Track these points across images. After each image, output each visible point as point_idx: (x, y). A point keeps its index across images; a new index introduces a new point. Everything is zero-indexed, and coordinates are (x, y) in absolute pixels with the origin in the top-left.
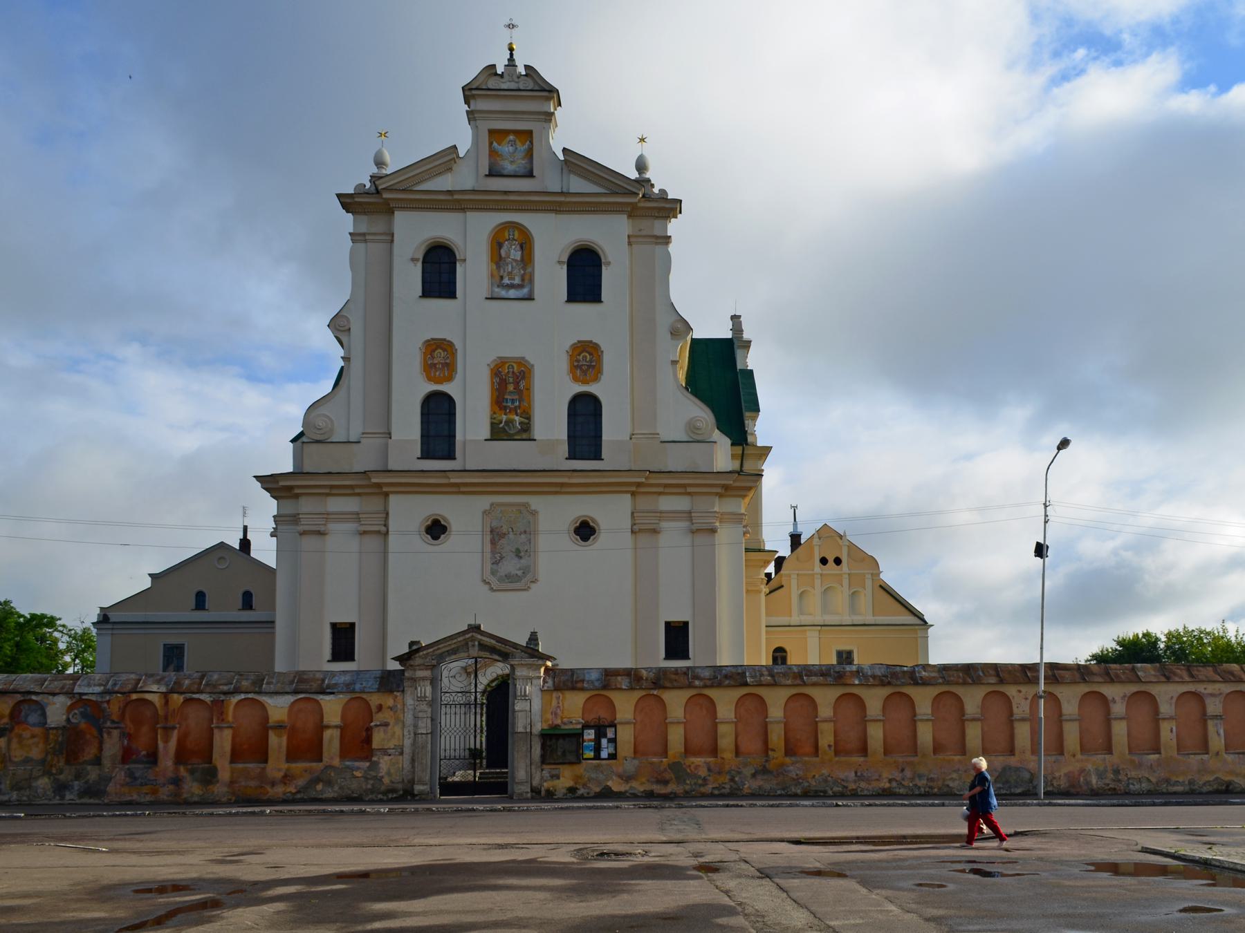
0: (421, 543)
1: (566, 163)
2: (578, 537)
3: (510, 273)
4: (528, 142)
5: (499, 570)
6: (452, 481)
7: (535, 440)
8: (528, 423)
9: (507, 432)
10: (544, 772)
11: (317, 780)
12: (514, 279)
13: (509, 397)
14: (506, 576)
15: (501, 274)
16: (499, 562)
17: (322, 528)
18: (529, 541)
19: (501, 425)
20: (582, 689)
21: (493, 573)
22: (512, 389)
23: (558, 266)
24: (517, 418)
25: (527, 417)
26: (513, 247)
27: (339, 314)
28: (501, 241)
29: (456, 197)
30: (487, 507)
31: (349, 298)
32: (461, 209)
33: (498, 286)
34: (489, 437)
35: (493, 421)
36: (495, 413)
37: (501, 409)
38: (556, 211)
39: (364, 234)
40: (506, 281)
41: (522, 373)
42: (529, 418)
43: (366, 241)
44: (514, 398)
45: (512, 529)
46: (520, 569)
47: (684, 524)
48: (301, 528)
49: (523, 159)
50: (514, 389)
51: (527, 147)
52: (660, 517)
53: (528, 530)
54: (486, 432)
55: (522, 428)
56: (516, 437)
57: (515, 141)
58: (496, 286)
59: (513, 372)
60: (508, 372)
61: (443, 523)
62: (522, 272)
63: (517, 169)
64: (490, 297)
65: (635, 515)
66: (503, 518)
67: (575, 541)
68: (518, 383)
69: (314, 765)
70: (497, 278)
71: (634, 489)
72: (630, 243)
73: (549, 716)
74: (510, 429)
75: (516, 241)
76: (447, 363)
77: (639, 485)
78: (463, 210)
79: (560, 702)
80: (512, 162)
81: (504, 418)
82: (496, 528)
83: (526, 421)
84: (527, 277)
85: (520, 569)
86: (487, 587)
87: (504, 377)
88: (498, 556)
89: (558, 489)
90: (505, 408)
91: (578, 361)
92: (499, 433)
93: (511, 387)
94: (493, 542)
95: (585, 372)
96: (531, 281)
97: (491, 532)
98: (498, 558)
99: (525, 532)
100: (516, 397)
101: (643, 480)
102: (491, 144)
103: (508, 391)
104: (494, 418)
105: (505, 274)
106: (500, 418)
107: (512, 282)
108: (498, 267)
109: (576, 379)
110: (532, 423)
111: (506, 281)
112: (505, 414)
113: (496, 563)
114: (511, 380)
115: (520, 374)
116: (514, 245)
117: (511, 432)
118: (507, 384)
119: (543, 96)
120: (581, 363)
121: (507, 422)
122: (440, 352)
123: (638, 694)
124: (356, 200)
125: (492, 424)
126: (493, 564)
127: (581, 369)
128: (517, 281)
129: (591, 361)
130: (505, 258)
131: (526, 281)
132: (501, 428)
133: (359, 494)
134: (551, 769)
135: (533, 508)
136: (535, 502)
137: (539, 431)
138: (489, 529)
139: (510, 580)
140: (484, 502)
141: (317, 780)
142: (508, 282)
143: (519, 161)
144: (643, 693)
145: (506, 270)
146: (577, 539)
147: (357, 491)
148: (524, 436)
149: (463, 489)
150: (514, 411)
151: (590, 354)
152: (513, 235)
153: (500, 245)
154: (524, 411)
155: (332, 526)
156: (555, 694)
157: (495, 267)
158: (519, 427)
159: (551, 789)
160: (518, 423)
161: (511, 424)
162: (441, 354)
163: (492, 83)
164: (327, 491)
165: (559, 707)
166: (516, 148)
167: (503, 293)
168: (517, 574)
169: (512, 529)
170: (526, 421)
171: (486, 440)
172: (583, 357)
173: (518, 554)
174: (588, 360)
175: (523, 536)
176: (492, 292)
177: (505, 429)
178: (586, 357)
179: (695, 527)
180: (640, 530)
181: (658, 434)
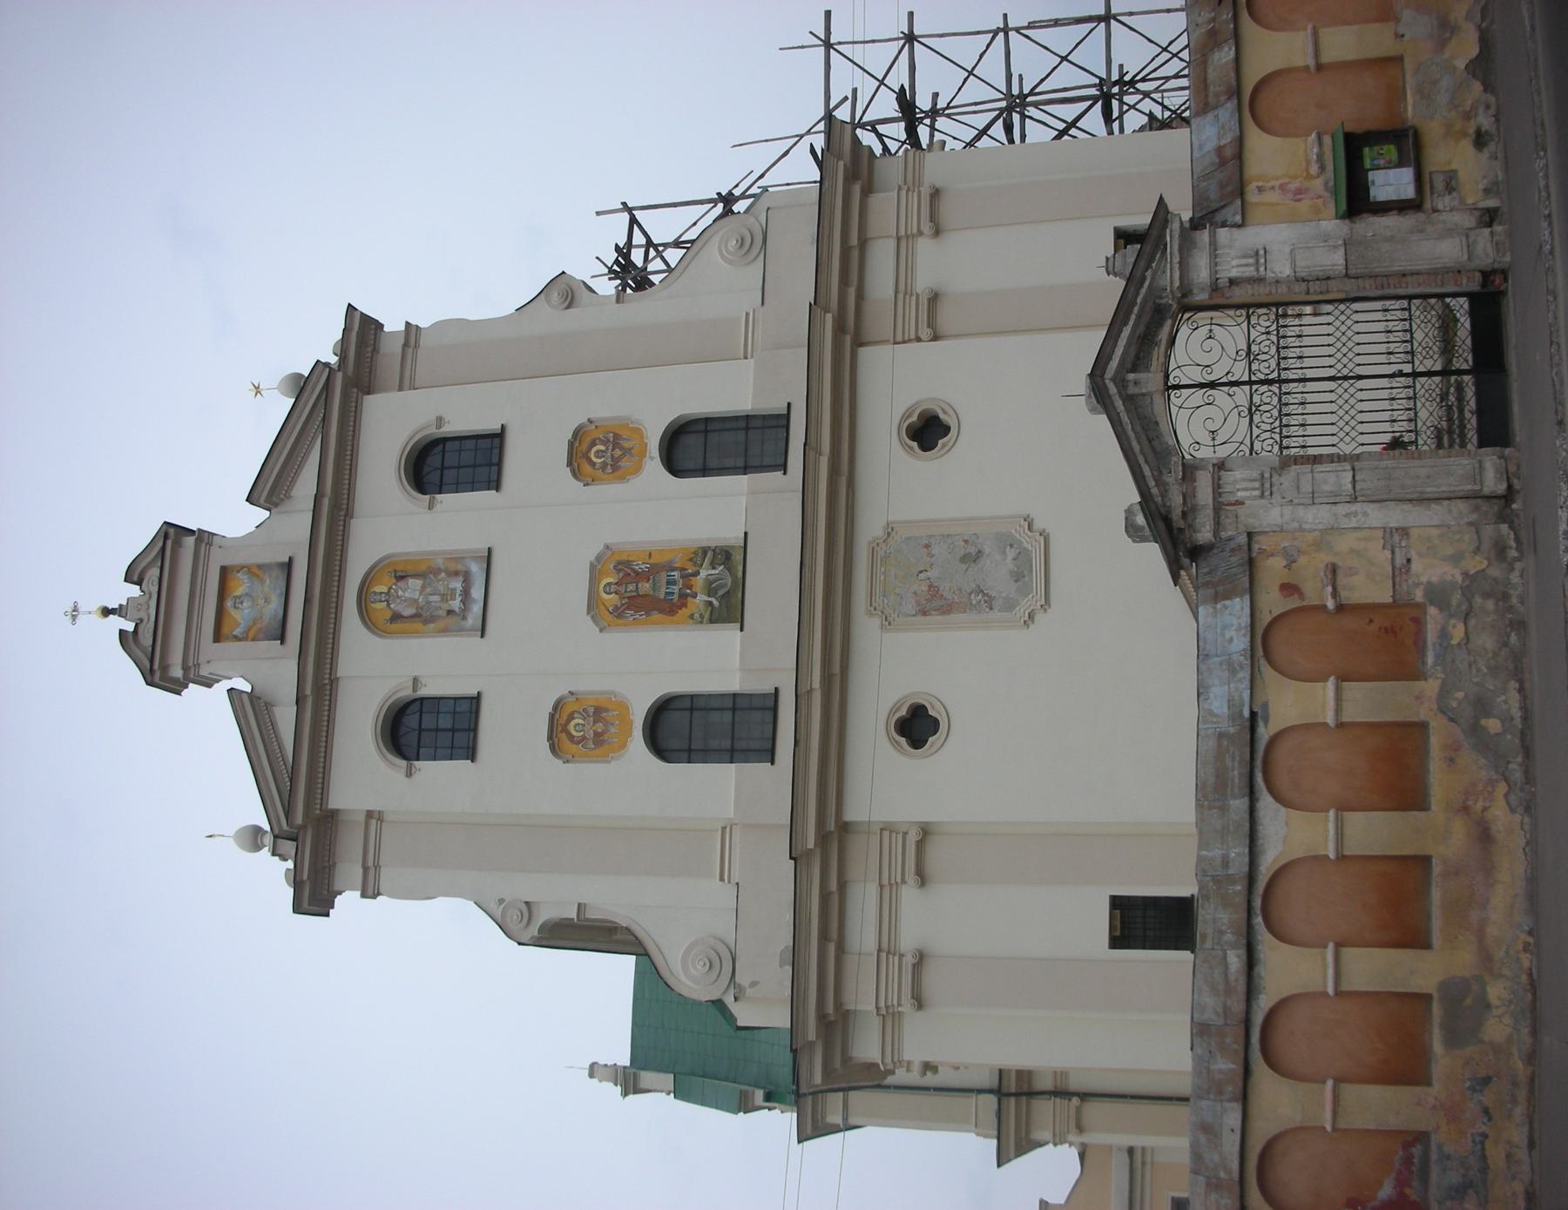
0: (943, 755)
1: (276, 505)
2: (940, 442)
3: (444, 598)
4: (239, 575)
5: (1004, 595)
6: (816, 684)
7: (746, 534)
8: (714, 551)
9: (729, 591)
10: (1440, 207)
11: (1475, 730)
13: (663, 590)
15: (444, 613)
16: (987, 595)
17: (909, 960)
18: (946, 537)
19: (716, 603)
20: (1240, 141)
22: (647, 585)
23: (438, 507)
24: (703, 573)
25: (703, 554)
26: (400, 593)
27: (500, 921)
28: (388, 615)
29: (308, 691)
30: (875, 622)
31: (472, 903)
32: (331, 685)
33: (464, 618)
34: (738, 625)
36: (692, 617)
37: (684, 605)
38: (349, 514)
39: (366, 869)
40: (456, 604)
41: (620, 567)
42: (705, 551)
43: (377, 867)
44: (664, 580)
45: (921, 572)
46: (1004, 553)
47: (924, 246)
48: (907, 1007)
49: (262, 581)
51: (246, 577)
52: (906, 294)
54: (728, 635)
55: (723, 564)
56: (740, 574)
57: (236, 597)
58: (463, 623)
59: (616, 584)
60: (616, 593)
61: (903, 712)
62: (443, 575)
63: (278, 591)
64: (480, 633)
65: (899, 338)
66: (897, 591)
67: (947, 448)
68: (637, 574)
69: (1435, 742)
70: (451, 620)
71: (848, 339)
72: (415, 389)
73: (1305, 205)
74: (725, 585)
75: (390, 588)
76: (594, 713)
77: (840, 329)
78: (334, 681)
79: (1270, 184)
80: (267, 601)
81: (702, 597)
82: (918, 604)
83: (710, 554)
84: (452, 566)
86: (1039, 617)
87: (626, 600)
88: (974, 599)
89: (843, 481)
90: (683, 596)
91: (604, 465)
93: (645, 587)
94: (947, 609)
95: (627, 452)
96: (458, 558)
97: (924, 613)
98: (980, 597)
100: (663, 577)
101: (829, 317)
102: (237, 638)
103: (651, 593)
104: (702, 616)
105: (446, 607)
106: (702, 607)
107: (458, 592)
108: (432, 619)
109: (638, 469)
110: (713, 545)
111: (456, 604)
112: (695, 595)
113: (990, 602)
114: (631, 587)
115: (620, 570)
116: (396, 592)
117: (729, 585)
118: (639, 595)
119: (173, 550)
120: (609, 461)
122: (575, 727)
123: (1247, 24)
124: (305, 877)
125: (711, 621)
127: (620, 458)
128: (457, 584)
129: (605, 442)
130: (417, 608)
131: (460, 567)
133: (843, 886)
134: (1432, 194)
135: (878, 532)
136: (870, 526)
137: (727, 532)
138: (921, 619)
139: (1025, 572)
140: (866, 629)
141: (1475, 730)
142: (459, 599)
143: (266, 589)
144: (1245, 17)
145: (438, 605)
146: (944, 446)
147: (833, 886)
148: (738, 558)
149: (836, 669)
151: (593, 444)
152: (381, 593)
153: (396, 617)
154: (691, 560)
155: (908, 941)
156: (1252, 197)
157: (432, 626)
159: (1481, 186)
160: (713, 572)
162: (578, 724)
163: (146, 640)
164: (832, 948)
165: (1282, 187)
166: (247, 594)
167: (477, 608)
168: (1014, 559)
170: (710, 554)
171: (742, 630)
172: (597, 457)
173: (973, 558)
174: (602, 448)
175: (935, 550)
176: (473, 629)
177: (723, 596)
178: (597, 452)
179: (927, 227)
180: (931, 323)
181: (747, 314)
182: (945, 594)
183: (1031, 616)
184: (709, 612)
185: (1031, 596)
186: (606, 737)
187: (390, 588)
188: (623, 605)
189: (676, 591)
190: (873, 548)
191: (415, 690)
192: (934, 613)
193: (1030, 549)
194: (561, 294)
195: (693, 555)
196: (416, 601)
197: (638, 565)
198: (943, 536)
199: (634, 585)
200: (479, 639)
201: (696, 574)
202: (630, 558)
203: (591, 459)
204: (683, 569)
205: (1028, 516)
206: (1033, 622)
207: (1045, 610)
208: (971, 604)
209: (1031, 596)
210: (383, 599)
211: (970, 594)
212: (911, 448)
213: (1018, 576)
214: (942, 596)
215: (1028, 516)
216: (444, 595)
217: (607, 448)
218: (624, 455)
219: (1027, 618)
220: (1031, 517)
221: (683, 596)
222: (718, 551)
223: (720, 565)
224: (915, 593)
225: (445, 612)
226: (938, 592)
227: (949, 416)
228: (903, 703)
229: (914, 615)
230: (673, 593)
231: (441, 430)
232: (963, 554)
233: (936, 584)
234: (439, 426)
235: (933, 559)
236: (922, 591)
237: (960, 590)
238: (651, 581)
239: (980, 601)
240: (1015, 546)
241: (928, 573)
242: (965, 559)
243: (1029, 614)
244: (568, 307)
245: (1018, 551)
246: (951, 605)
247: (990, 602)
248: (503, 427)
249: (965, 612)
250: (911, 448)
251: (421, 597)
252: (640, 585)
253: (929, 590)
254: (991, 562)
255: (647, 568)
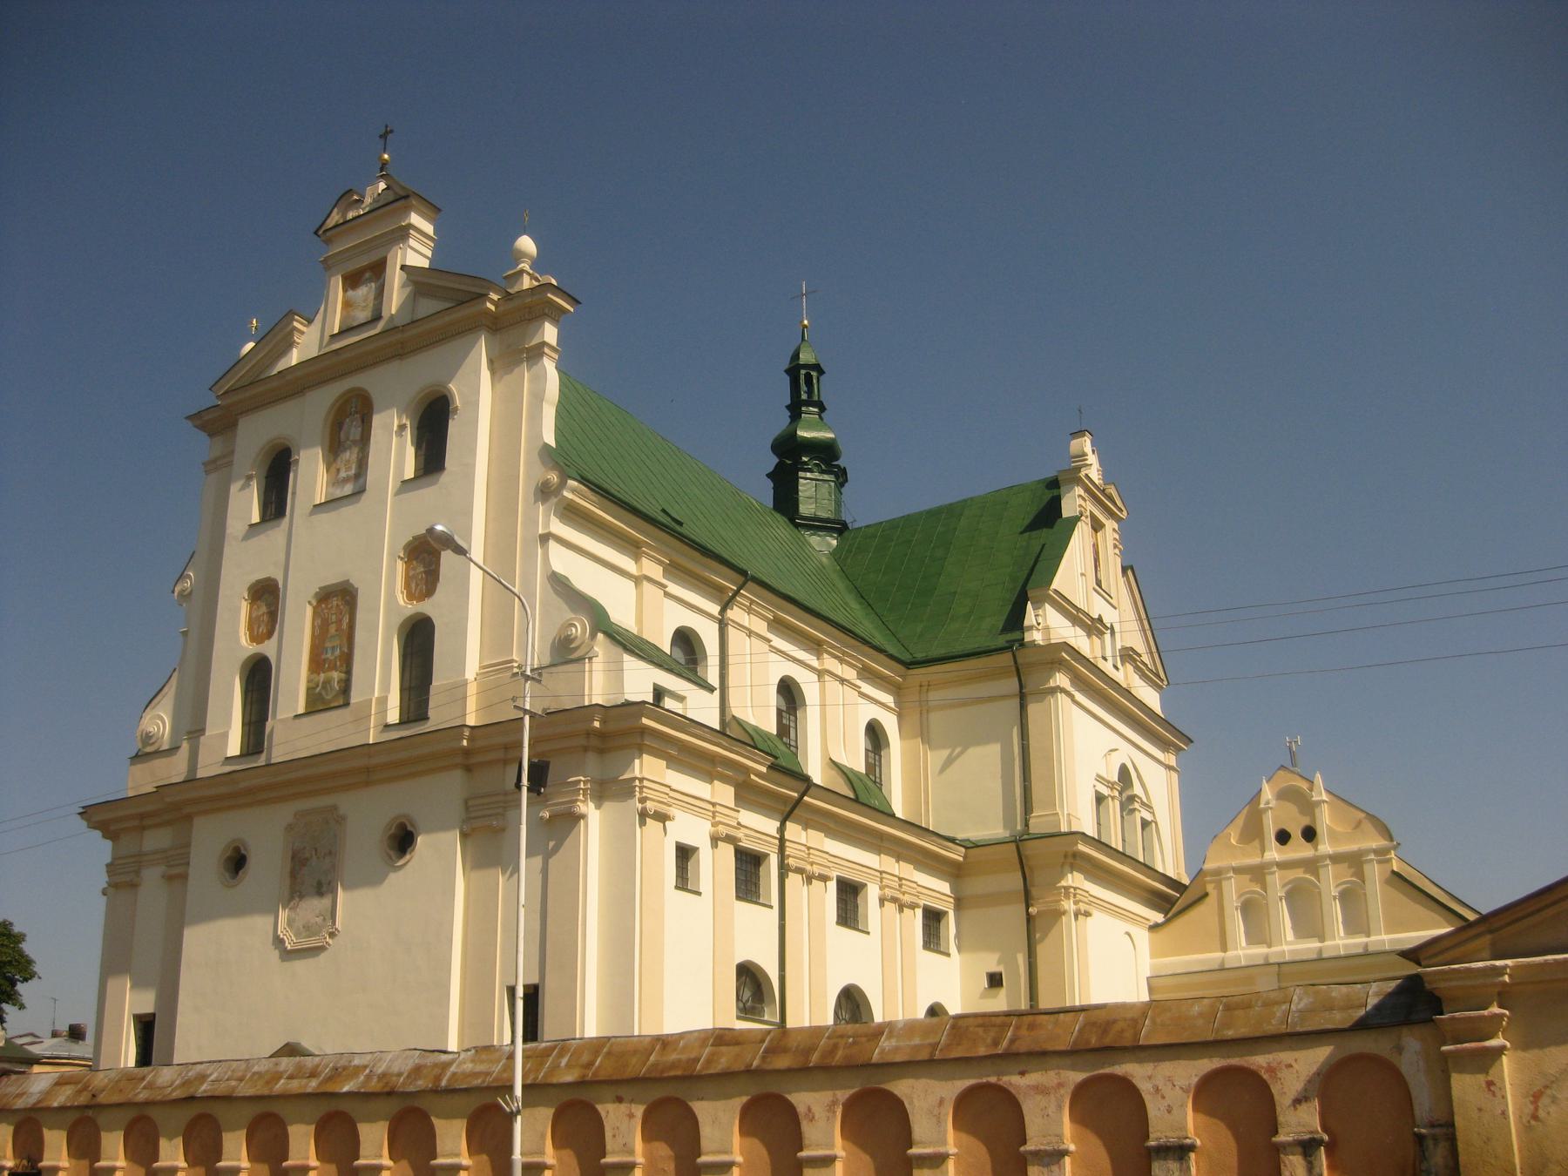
19: (318, 689)
26: (354, 423)
45: (316, 851)
50: (336, 631)
56: (332, 705)
65: (470, 803)
74: (327, 695)
92: (318, 703)
99: (330, 853)
117: (329, 697)
121: (327, 683)
124: (206, 418)
138: (290, 853)
140: (284, 813)
196: (348, 439)
213: (307, 927)
250: (390, 829)
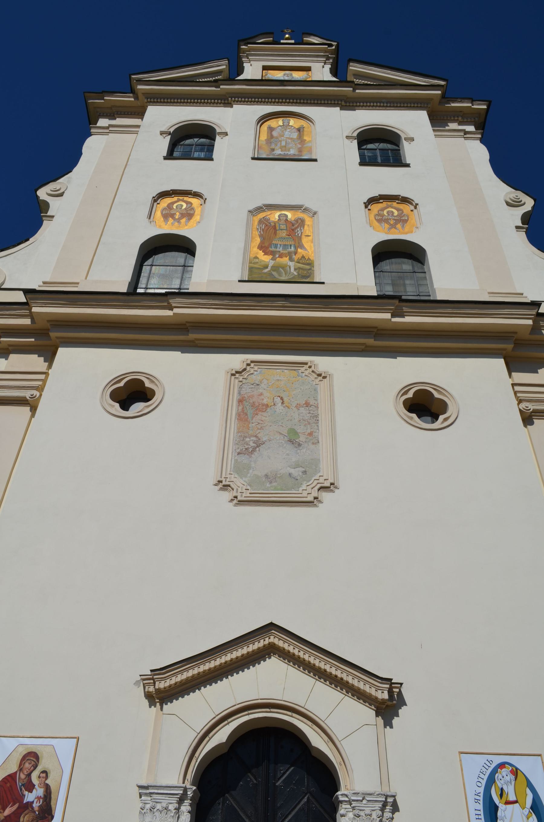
2: (414, 416)
5: (253, 465)
7: (323, 283)
12: (289, 151)
14: (266, 476)
16: (254, 450)
18: (316, 418)
19: (266, 270)
21: (240, 470)
23: (347, 142)
24: (292, 264)
26: (288, 130)
35: (252, 265)
41: (300, 221)
42: (310, 264)
45: (282, 399)
46: (297, 466)
53: (312, 402)
55: (299, 274)
59: (287, 220)
61: (148, 384)
62: (300, 146)
64: (256, 156)
81: (272, 263)
82: (252, 396)
83: (308, 267)
85: (297, 466)
94: (242, 417)
97: (240, 401)
98: (252, 444)
99: (307, 404)
112: (272, 259)
114: (283, 227)
126: (239, 454)
132: (265, 273)
135: (321, 369)
138: (236, 397)
139: (274, 484)
146: (412, 418)
150: (290, 256)
158: (296, 273)
161: (281, 269)
162: (182, 206)
169: (282, 399)
170: (308, 267)
171: (240, 281)
172: (388, 212)
182: (259, 417)
183: (226, 487)
184: (260, 267)
185: (248, 487)
186: (171, 220)
187: (292, 126)
188: (270, 223)
189: (278, 249)
190: (306, 364)
191: (220, 133)
192: (240, 408)
193: (301, 489)
194: (518, 198)
195: (307, 258)
197: (301, 230)
198: (317, 416)
199: (285, 228)
200: (251, 155)
201: (291, 259)
202: (306, 226)
203: (386, 209)
204: (296, 253)
205: (336, 488)
206: (221, 489)
207: (232, 500)
208: (246, 437)
209: (248, 487)
210: (285, 124)
211: (256, 436)
212: (406, 393)
214: (257, 414)
215: (336, 488)
216: (286, 147)
217: (395, 216)
218: (391, 225)
219: (224, 483)
220: (336, 490)
221: (273, 253)
222: (309, 271)
223: (298, 273)
224: (261, 394)
225: (274, 148)
226: (260, 411)
227: (443, 422)
228: (157, 385)
229: (239, 393)
230: (277, 248)
231: (404, 141)
232: (298, 431)
233: (268, 410)
234: (406, 139)
235: (295, 409)
236: (263, 399)
237: (261, 428)
238: (287, 237)
239: (247, 444)
240: (304, 476)
241: (280, 404)
242: (293, 432)
243: (229, 486)
244: (508, 204)
245: (299, 478)
246: (246, 420)
247: (249, 452)
248: (408, 165)
249: (238, 432)
251: (285, 138)
252: (285, 231)
253: (263, 405)
254: (288, 455)
255: (298, 234)
